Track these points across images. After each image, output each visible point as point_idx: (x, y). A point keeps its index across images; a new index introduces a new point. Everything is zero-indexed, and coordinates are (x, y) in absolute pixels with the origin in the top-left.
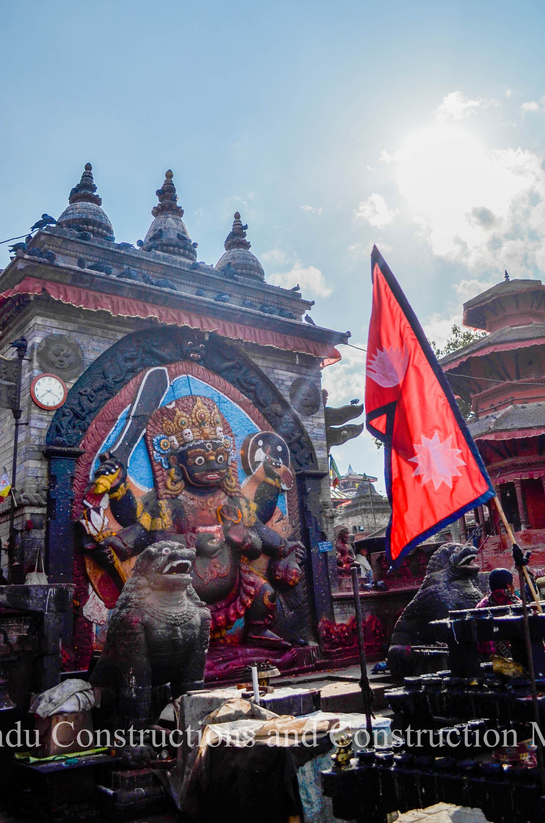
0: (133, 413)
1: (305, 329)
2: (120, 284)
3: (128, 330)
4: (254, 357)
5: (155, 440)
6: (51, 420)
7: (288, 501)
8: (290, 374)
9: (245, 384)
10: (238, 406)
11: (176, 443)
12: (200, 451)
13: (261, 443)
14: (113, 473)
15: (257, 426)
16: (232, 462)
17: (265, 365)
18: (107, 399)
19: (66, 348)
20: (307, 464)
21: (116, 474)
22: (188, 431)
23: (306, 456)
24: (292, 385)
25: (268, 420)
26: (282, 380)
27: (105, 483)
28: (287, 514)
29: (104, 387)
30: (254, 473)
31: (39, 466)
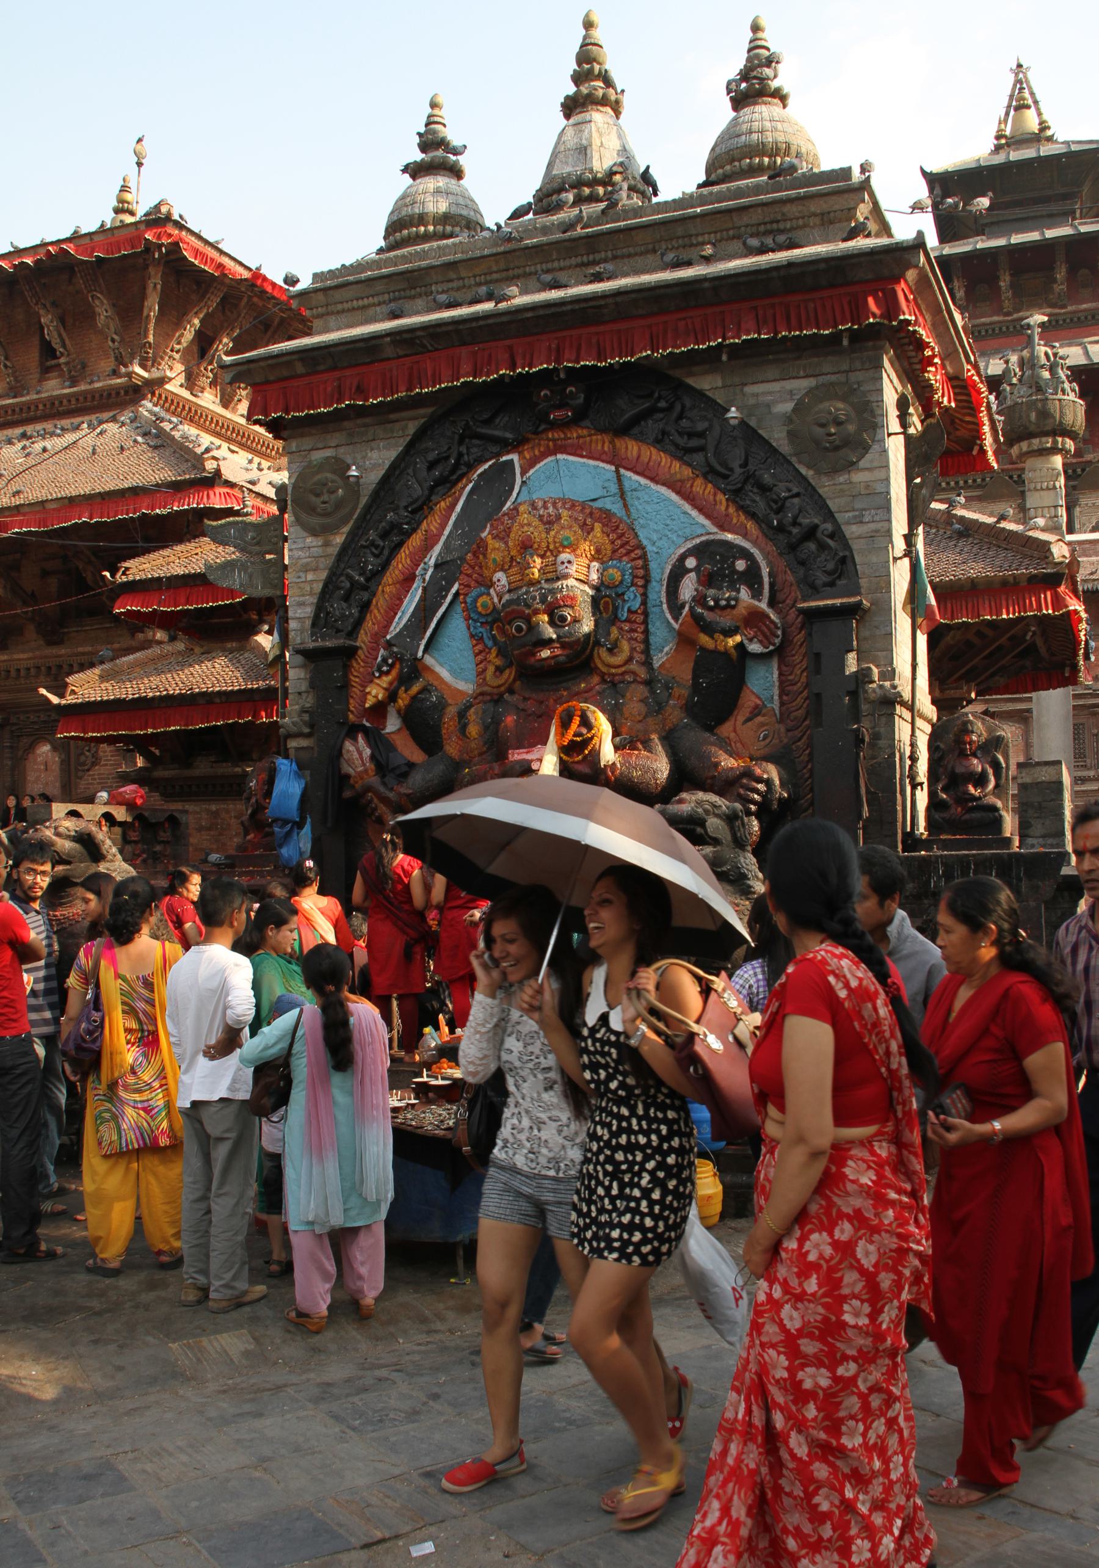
0: (432, 562)
1: (782, 273)
2: (374, 342)
3: (422, 411)
4: (691, 374)
5: (469, 600)
6: (314, 600)
7: (780, 674)
8: (790, 385)
9: (682, 441)
10: (663, 490)
11: (496, 600)
12: (513, 611)
13: (691, 562)
14: (387, 673)
15: (707, 522)
16: (629, 611)
17: (720, 384)
18: (400, 544)
19: (329, 475)
20: (832, 584)
21: (394, 673)
22: (500, 575)
23: (830, 566)
24: (794, 410)
25: (734, 502)
26: (768, 406)
27: (376, 692)
28: (776, 705)
29: (394, 527)
30: (676, 626)
31: (302, 676)
